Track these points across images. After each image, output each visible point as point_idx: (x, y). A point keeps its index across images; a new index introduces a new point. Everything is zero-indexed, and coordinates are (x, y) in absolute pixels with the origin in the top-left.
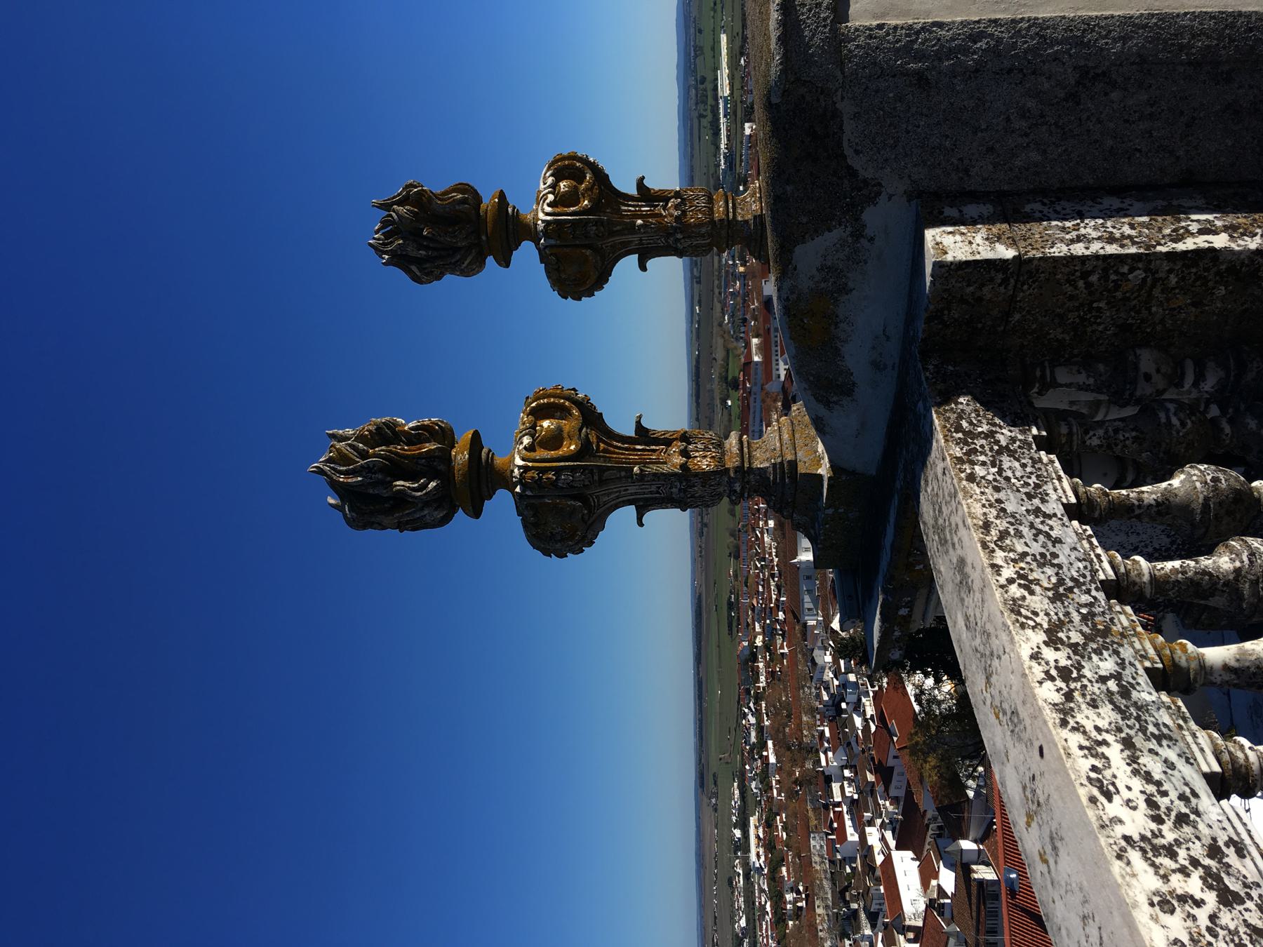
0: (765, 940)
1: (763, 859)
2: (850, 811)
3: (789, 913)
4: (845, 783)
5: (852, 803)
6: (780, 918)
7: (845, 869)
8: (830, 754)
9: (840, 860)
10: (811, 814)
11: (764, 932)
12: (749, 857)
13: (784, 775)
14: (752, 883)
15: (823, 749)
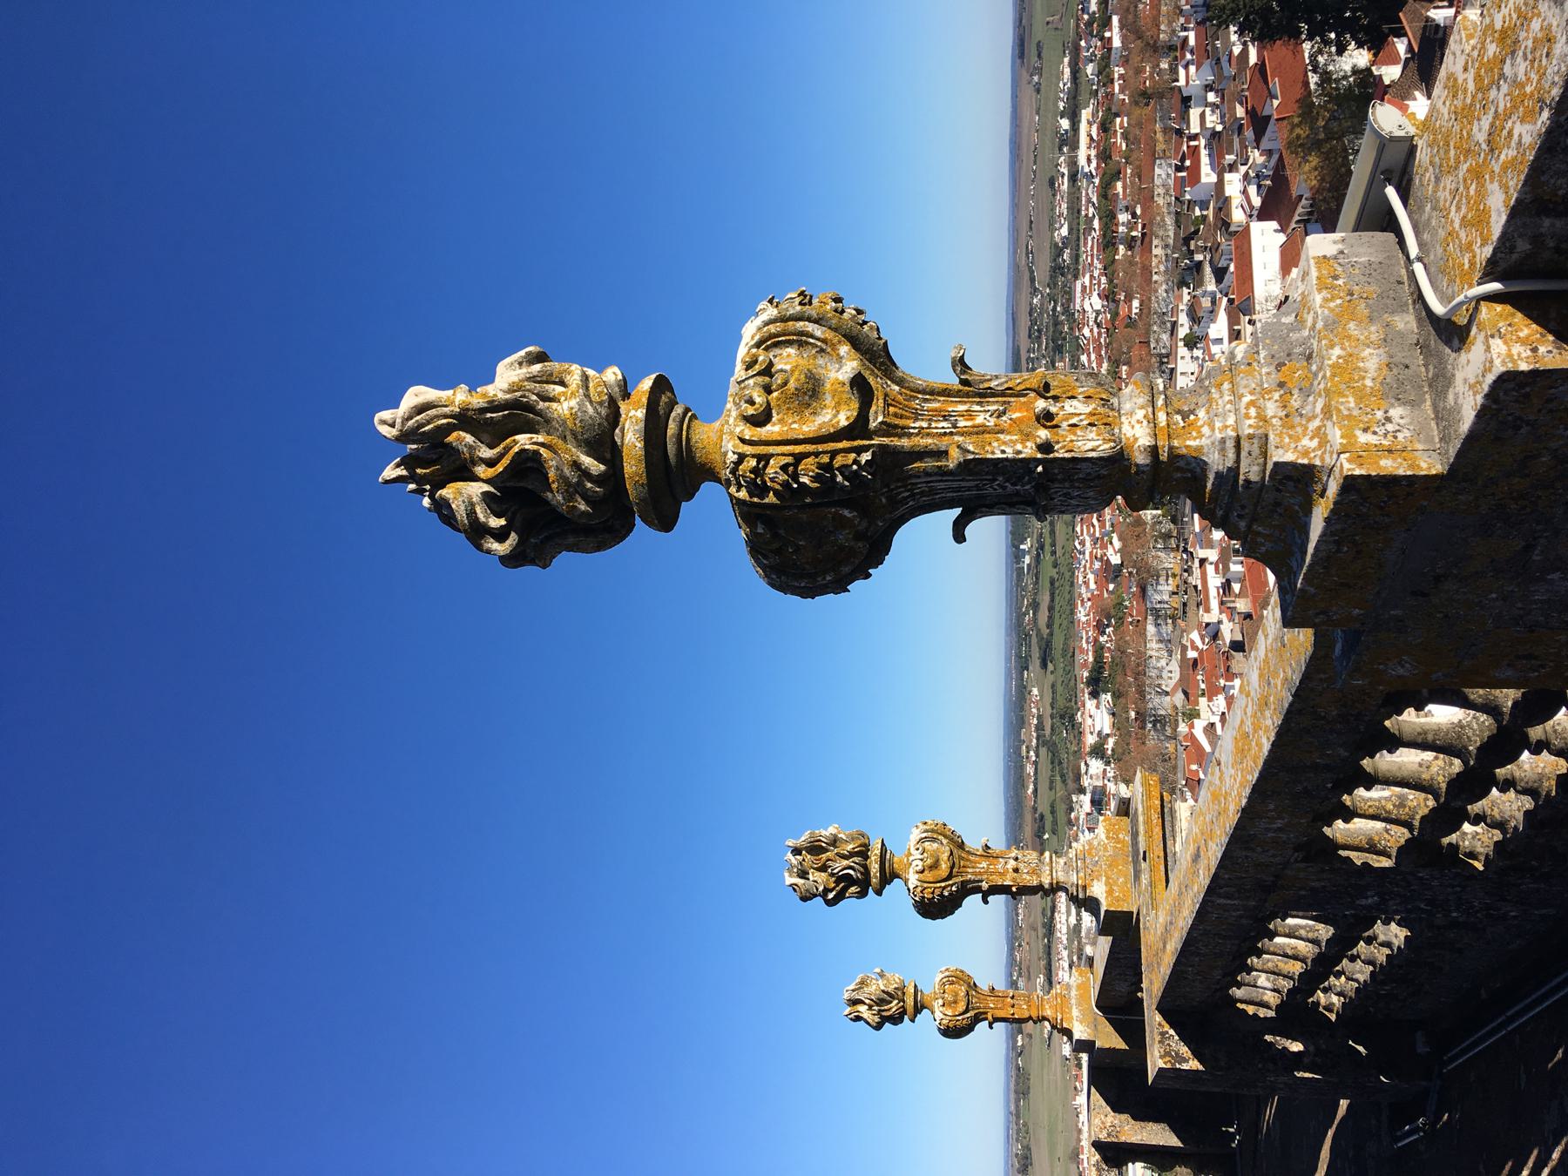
0: (1089, 258)
1: (1094, 164)
2: (1209, 146)
3: (1120, 236)
4: (1208, 110)
5: (1215, 135)
6: (1108, 242)
7: (1194, 211)
8: (1192, 69)
9: (1189, 201)
10: (1159, 136)
11: (1089, 249)
12: (1076, 157)
13: (1131, 73)
14: (1079, 189)
15: (1184, 62)
